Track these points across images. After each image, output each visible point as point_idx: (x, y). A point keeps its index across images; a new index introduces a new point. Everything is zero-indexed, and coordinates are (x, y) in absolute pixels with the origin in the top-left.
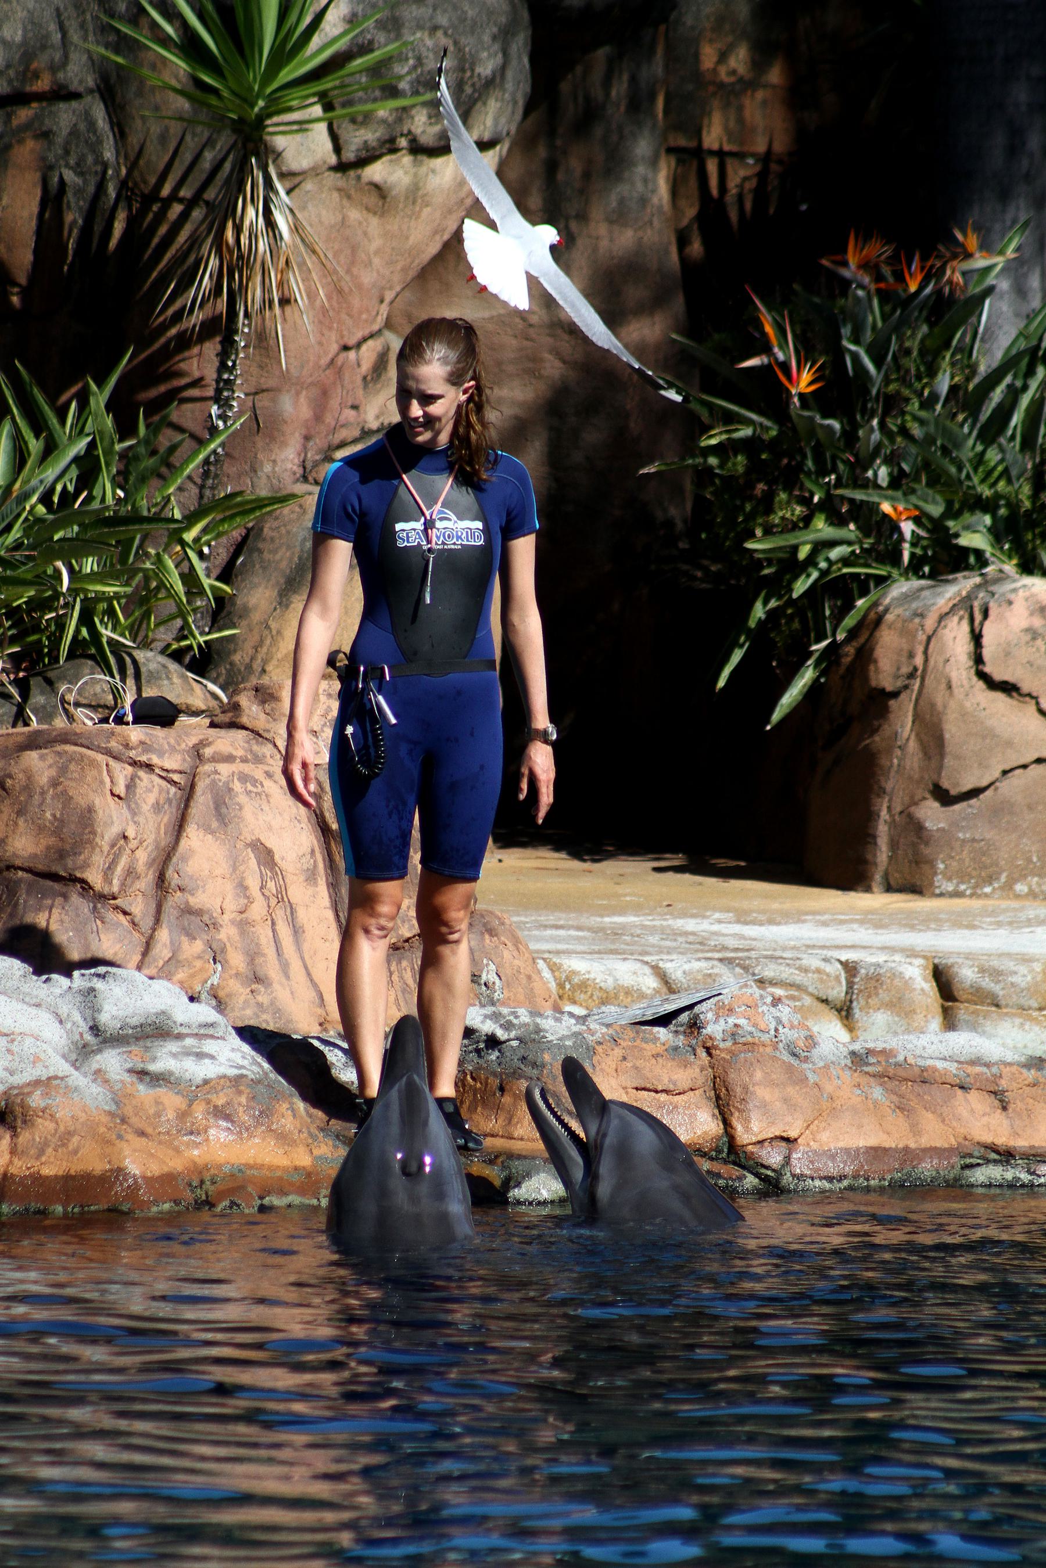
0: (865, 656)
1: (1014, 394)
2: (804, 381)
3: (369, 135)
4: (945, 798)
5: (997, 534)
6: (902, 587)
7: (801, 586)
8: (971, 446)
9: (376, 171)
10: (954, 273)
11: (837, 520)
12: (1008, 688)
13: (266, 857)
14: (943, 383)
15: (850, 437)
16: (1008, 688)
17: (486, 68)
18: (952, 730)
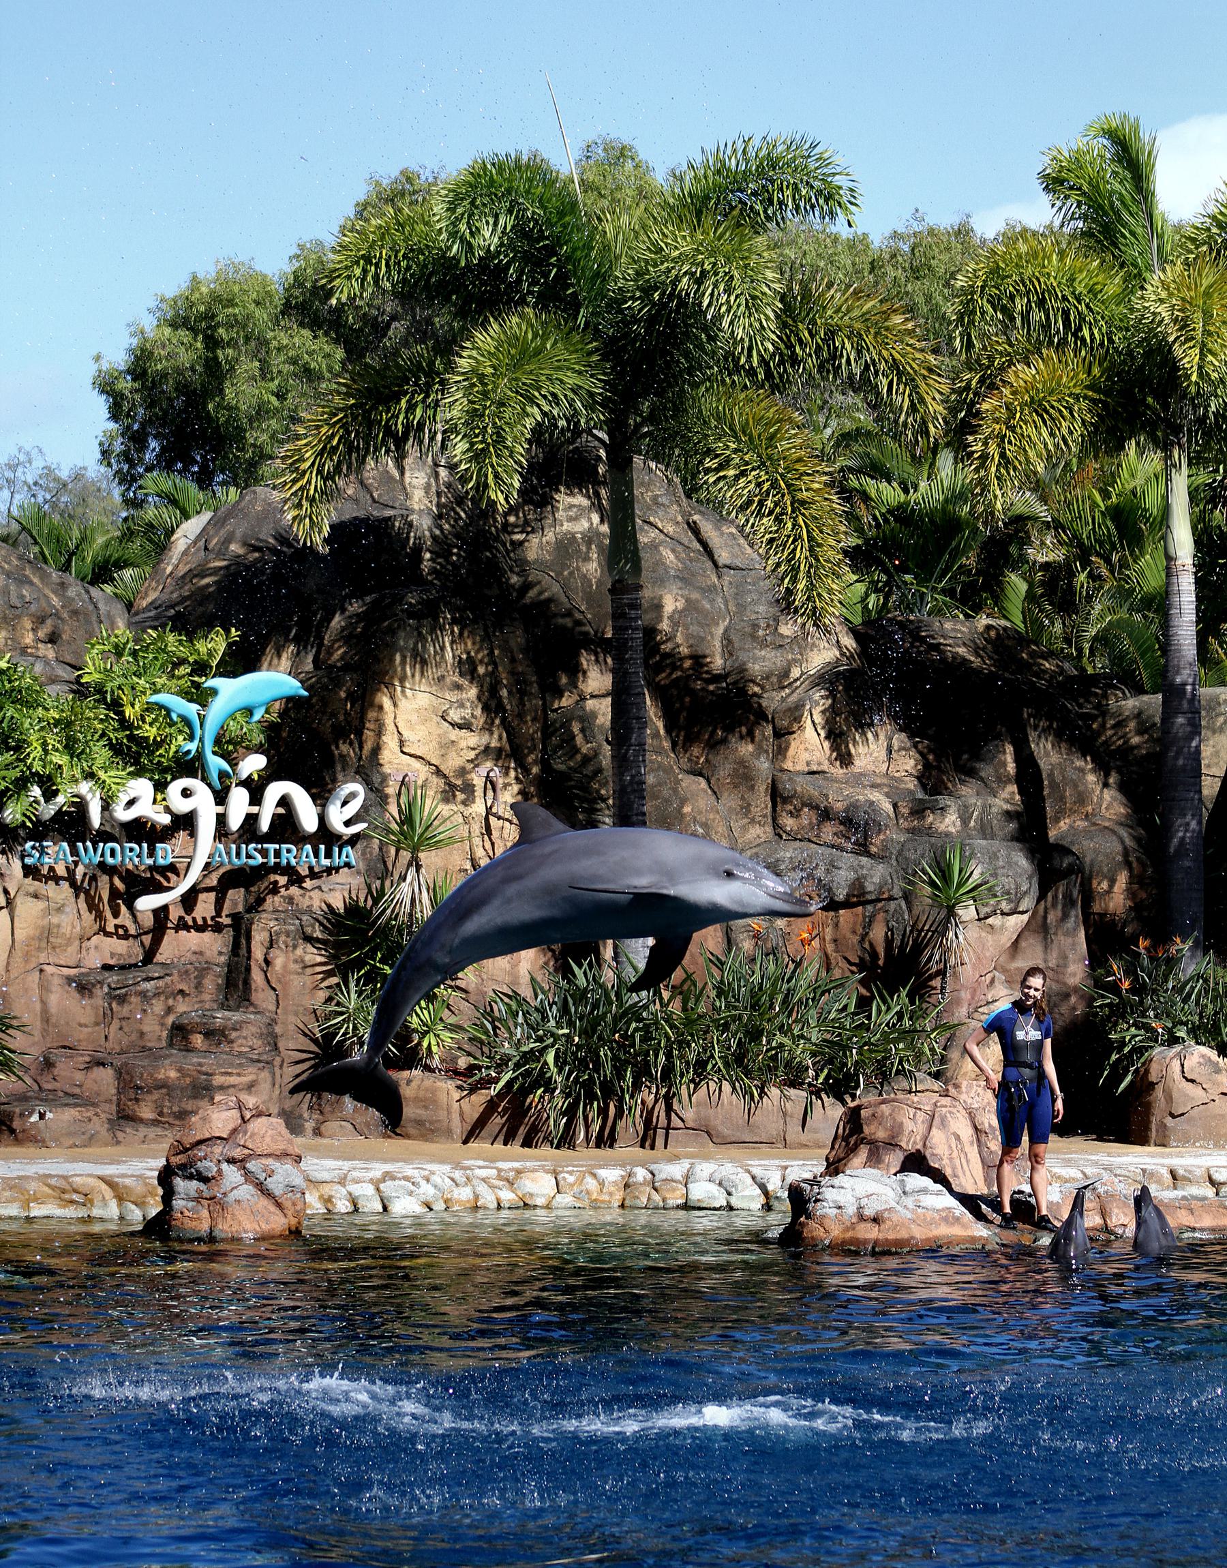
0: (1147, 1071)
1: (1193, 988)
2: (1126, 985)
3: (988, 910)
4: (1173, 1116)
5: (1188, 1033)
6: (1158, 1049)
7: (1126, 1050)
8: (1181, 1005)
9: (990, 921)
10: (1173, 950)
11: (1138, 1028)
12: (1192, 1081)
13: (958, 1138)
14: (1170, 985)
15: (1141, 1002)
16: (1192, 1081)
17: (1024, 888)
18: (1175, 1095)
